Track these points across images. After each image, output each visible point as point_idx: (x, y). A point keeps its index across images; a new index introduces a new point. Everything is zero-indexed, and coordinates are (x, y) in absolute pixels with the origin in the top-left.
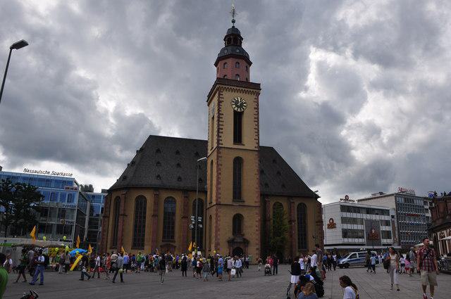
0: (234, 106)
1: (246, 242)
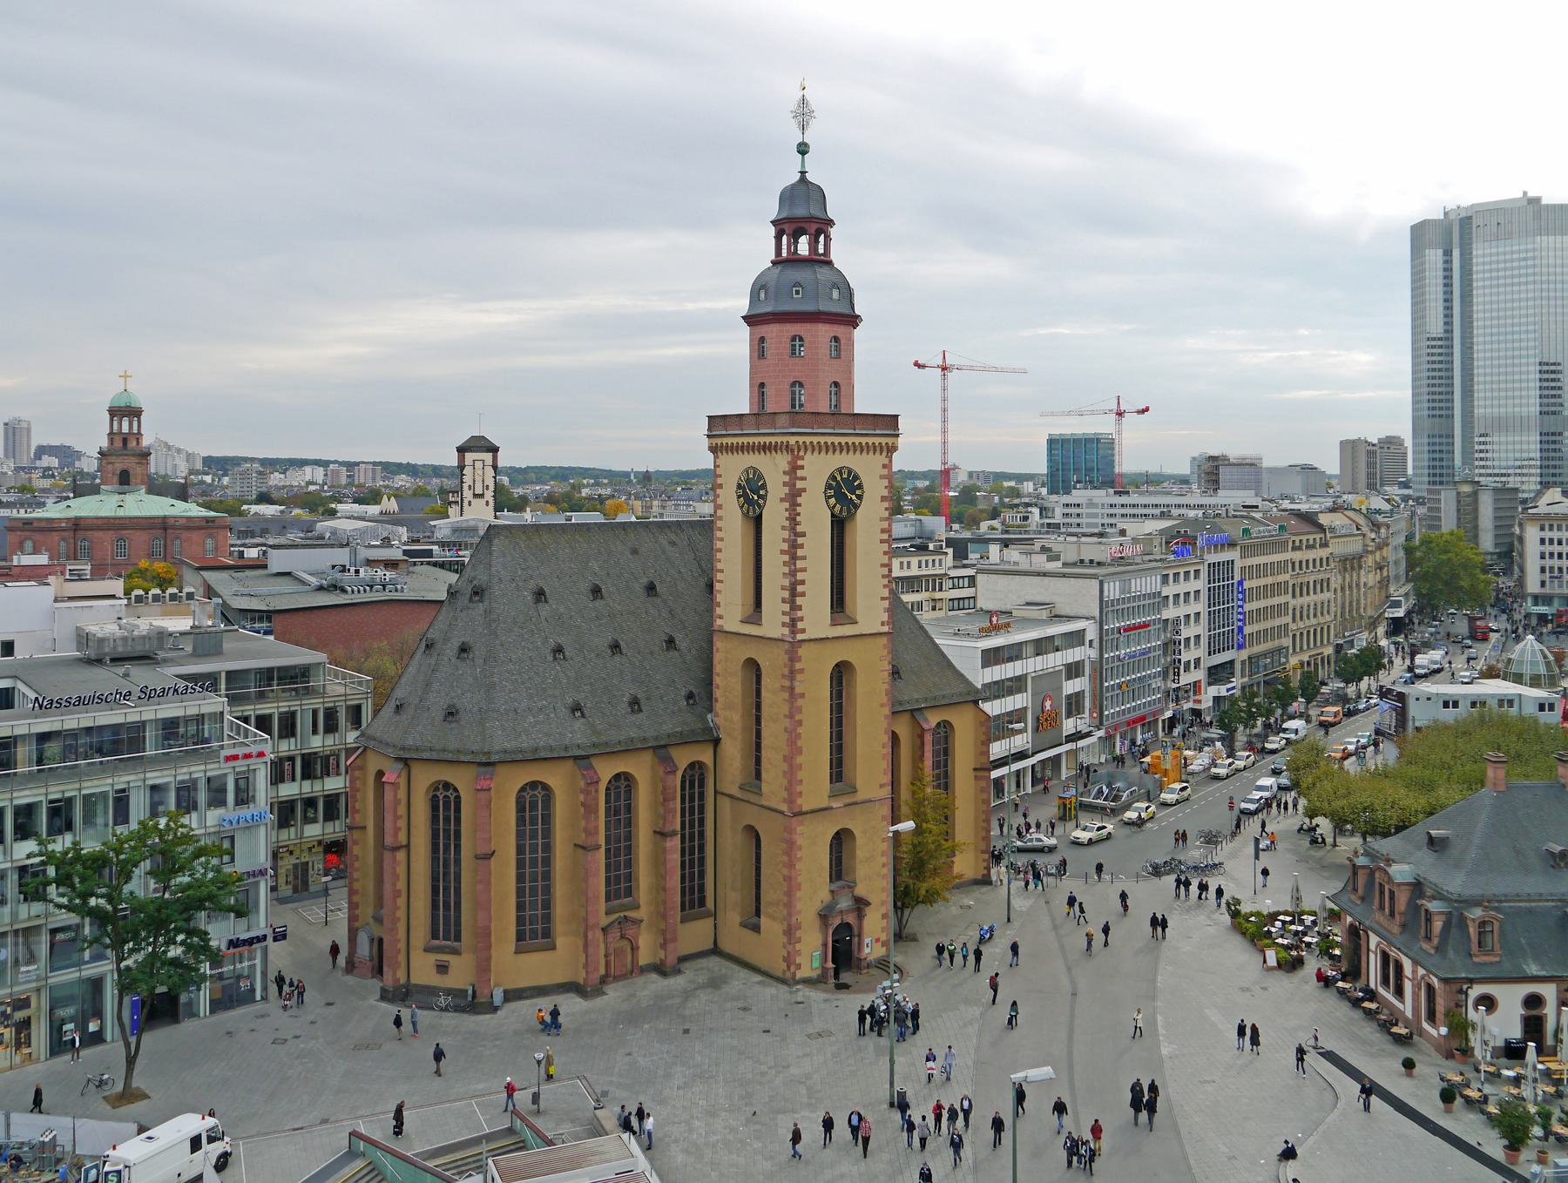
0: (833, 501)
1: (861, 904)
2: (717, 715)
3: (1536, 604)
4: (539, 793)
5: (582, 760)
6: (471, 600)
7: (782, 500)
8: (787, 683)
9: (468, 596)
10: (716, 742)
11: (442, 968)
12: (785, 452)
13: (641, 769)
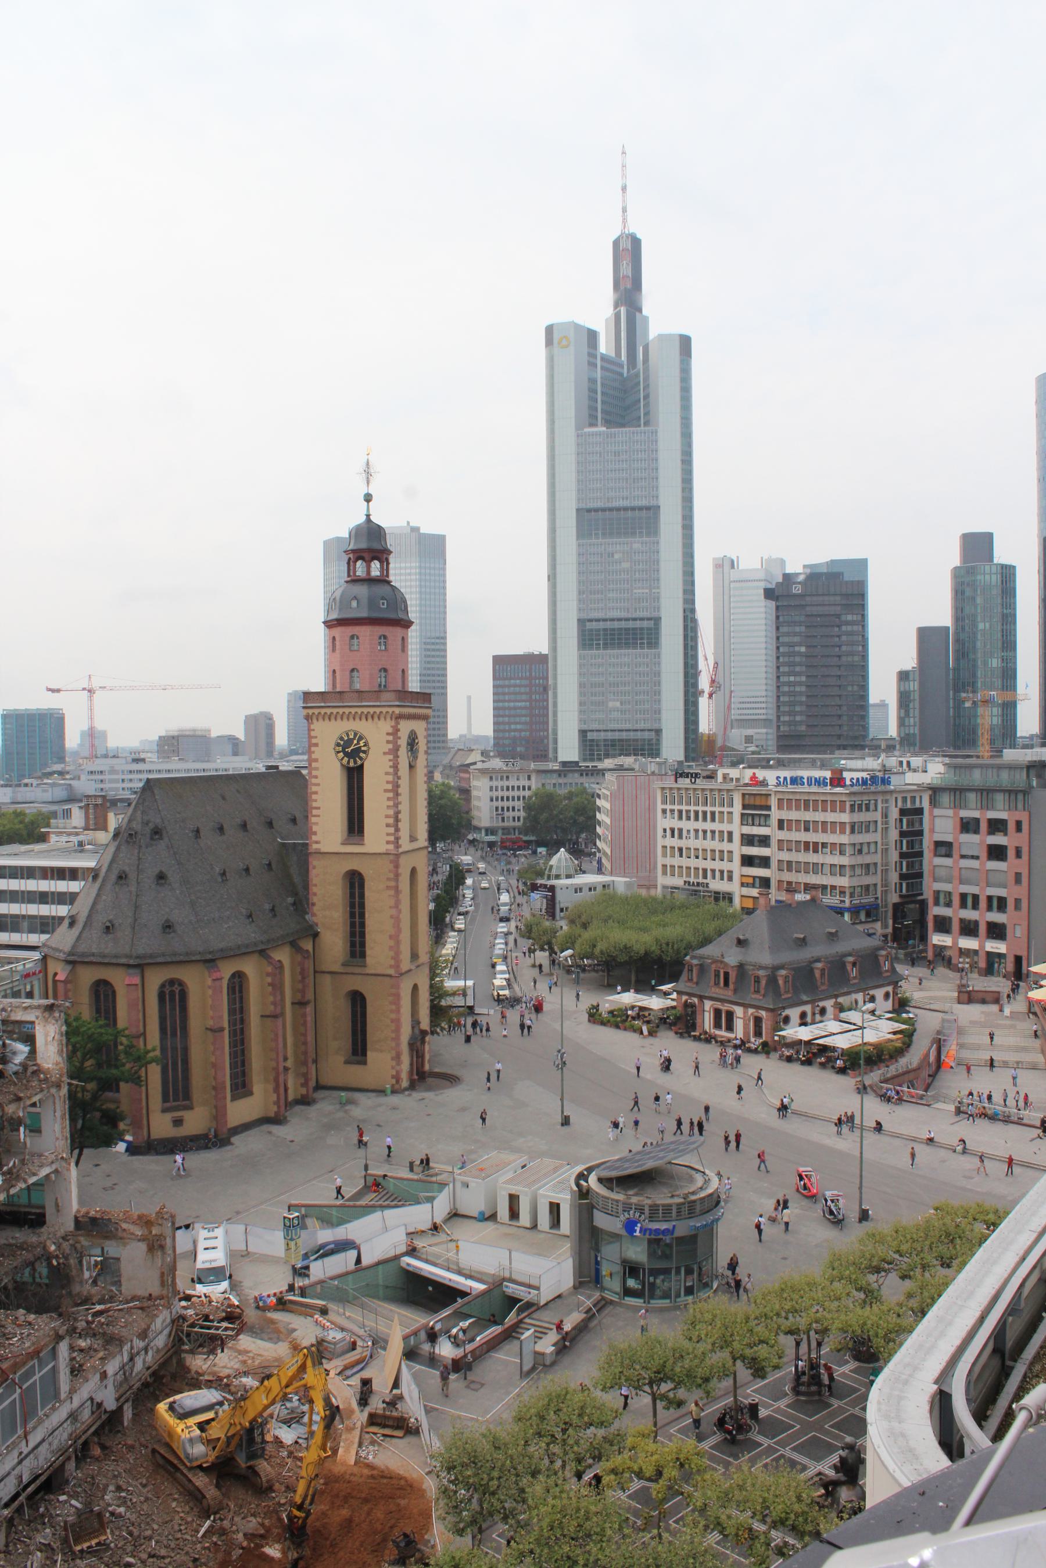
2: (314, 915)
3: (487, 835)
4: (236, 980)
5: (262, 953)
6: (152, 839)
7: (385, 753)
8: (393, 884)
9: (148, 836)
10: (316, 935)
11: (178, 1122)
12: (388, 719)
13: (283, 956)
